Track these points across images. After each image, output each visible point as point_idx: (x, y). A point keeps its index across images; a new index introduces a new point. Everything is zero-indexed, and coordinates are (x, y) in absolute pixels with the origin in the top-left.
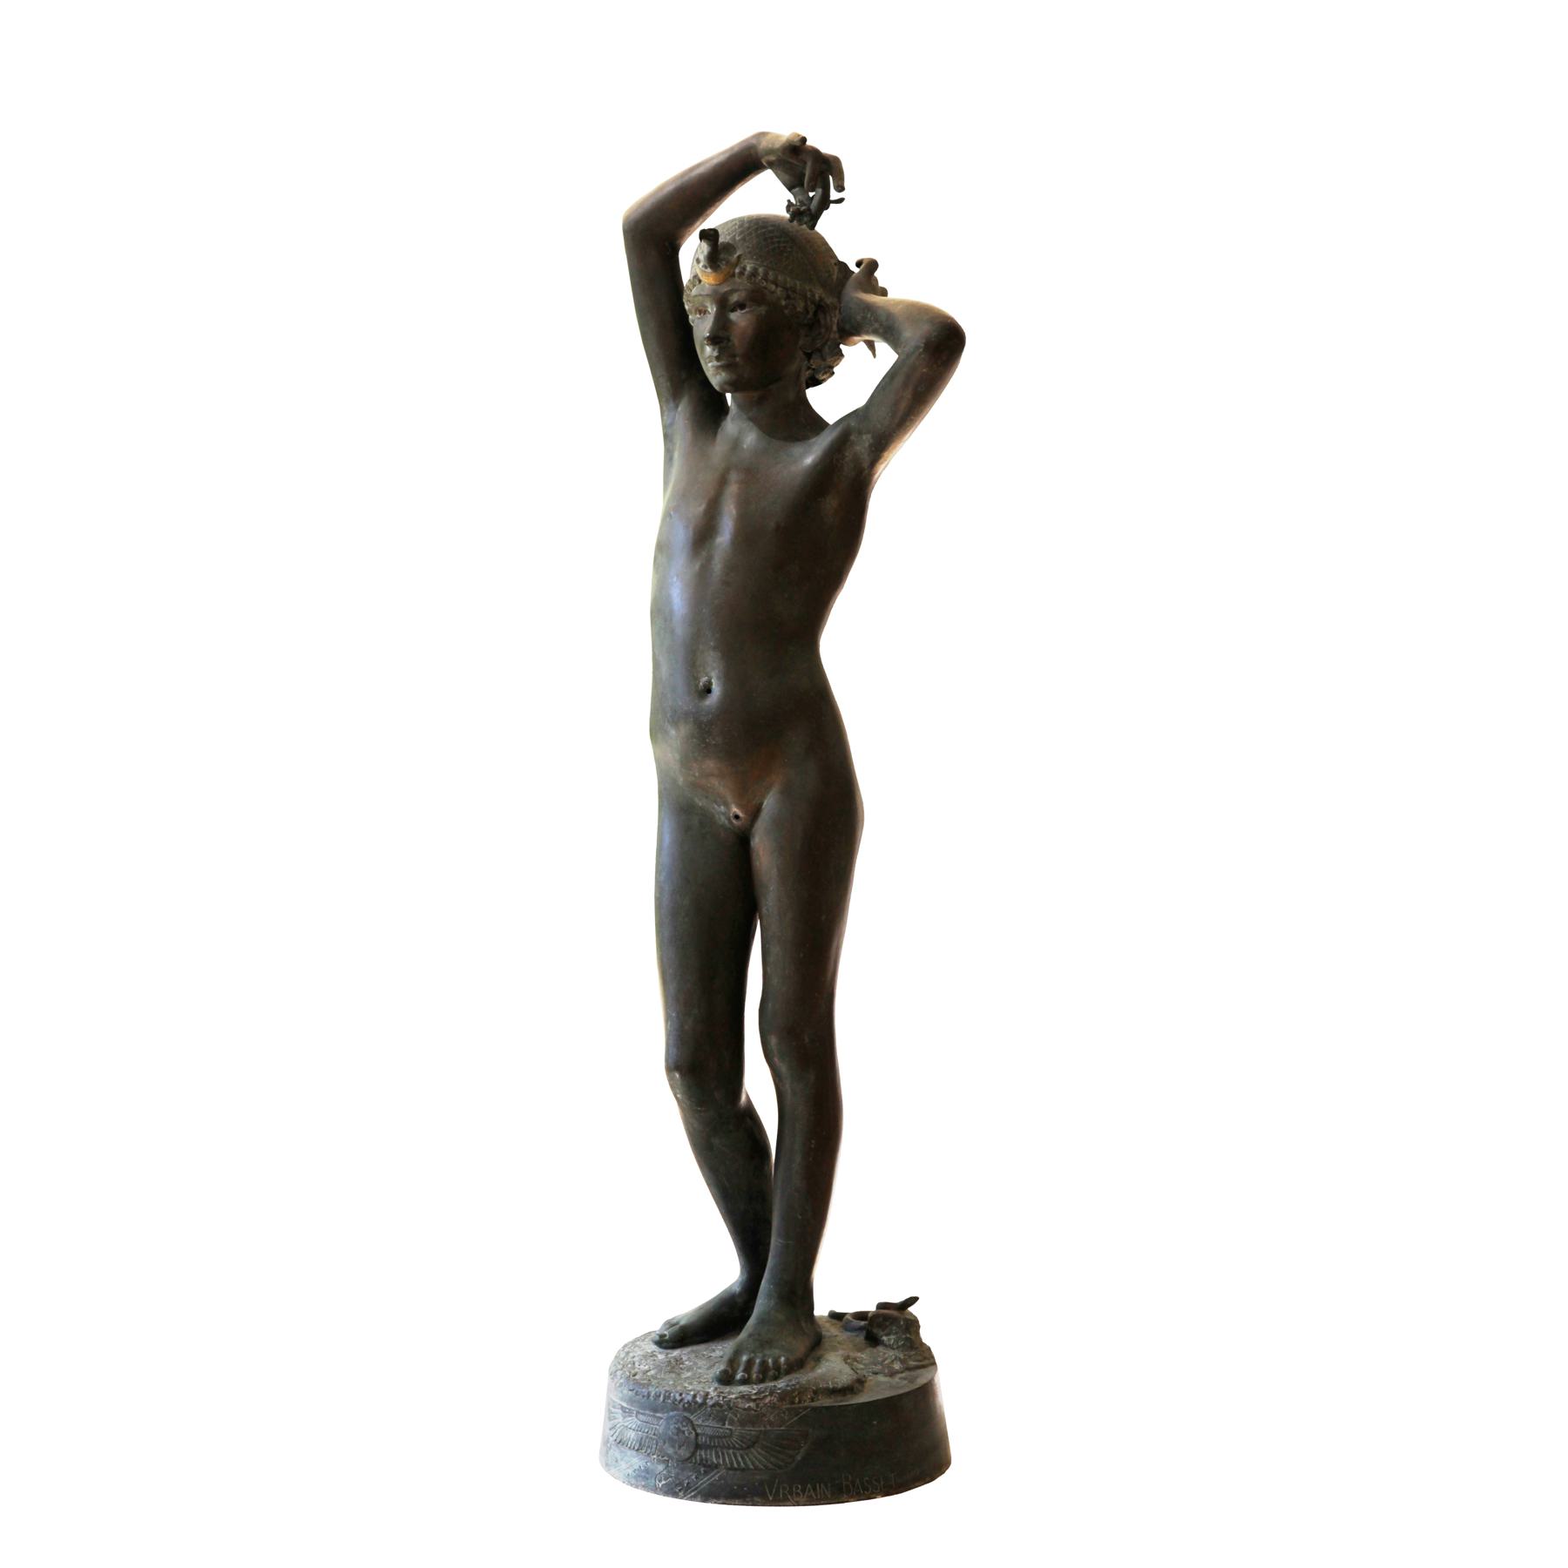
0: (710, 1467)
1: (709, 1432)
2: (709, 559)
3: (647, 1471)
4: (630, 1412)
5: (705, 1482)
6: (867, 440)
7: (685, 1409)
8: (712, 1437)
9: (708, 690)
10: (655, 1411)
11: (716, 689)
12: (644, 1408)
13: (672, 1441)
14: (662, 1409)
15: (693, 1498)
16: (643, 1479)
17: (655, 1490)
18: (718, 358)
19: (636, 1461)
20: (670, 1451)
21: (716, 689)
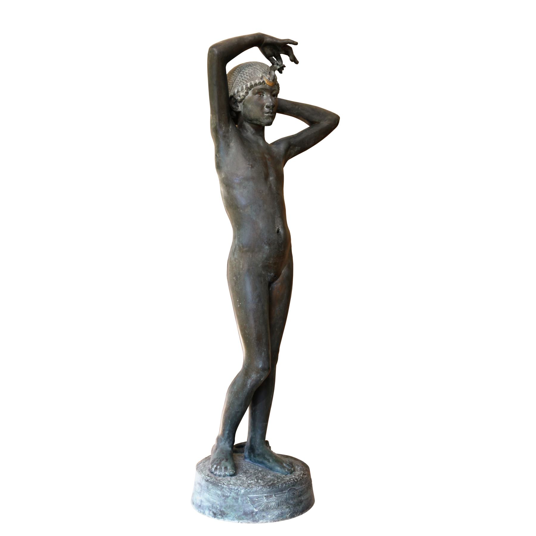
0: (301, 502)
2: (271, 185)
3: (282, 513)
4: (271, 496)
5: (300, 508)
6: (297, 148)
7: (293, 486)
8: (301, 492)
9: (278, 231)
10: (282, 491)
12: (277, 492)
13: (292, 499)
14: (285, 488)
15: (299, 515)
16: (282, 517)
17: (286, 518)
18: (272, 113)
20: (292, 502)
21: (281, 231)
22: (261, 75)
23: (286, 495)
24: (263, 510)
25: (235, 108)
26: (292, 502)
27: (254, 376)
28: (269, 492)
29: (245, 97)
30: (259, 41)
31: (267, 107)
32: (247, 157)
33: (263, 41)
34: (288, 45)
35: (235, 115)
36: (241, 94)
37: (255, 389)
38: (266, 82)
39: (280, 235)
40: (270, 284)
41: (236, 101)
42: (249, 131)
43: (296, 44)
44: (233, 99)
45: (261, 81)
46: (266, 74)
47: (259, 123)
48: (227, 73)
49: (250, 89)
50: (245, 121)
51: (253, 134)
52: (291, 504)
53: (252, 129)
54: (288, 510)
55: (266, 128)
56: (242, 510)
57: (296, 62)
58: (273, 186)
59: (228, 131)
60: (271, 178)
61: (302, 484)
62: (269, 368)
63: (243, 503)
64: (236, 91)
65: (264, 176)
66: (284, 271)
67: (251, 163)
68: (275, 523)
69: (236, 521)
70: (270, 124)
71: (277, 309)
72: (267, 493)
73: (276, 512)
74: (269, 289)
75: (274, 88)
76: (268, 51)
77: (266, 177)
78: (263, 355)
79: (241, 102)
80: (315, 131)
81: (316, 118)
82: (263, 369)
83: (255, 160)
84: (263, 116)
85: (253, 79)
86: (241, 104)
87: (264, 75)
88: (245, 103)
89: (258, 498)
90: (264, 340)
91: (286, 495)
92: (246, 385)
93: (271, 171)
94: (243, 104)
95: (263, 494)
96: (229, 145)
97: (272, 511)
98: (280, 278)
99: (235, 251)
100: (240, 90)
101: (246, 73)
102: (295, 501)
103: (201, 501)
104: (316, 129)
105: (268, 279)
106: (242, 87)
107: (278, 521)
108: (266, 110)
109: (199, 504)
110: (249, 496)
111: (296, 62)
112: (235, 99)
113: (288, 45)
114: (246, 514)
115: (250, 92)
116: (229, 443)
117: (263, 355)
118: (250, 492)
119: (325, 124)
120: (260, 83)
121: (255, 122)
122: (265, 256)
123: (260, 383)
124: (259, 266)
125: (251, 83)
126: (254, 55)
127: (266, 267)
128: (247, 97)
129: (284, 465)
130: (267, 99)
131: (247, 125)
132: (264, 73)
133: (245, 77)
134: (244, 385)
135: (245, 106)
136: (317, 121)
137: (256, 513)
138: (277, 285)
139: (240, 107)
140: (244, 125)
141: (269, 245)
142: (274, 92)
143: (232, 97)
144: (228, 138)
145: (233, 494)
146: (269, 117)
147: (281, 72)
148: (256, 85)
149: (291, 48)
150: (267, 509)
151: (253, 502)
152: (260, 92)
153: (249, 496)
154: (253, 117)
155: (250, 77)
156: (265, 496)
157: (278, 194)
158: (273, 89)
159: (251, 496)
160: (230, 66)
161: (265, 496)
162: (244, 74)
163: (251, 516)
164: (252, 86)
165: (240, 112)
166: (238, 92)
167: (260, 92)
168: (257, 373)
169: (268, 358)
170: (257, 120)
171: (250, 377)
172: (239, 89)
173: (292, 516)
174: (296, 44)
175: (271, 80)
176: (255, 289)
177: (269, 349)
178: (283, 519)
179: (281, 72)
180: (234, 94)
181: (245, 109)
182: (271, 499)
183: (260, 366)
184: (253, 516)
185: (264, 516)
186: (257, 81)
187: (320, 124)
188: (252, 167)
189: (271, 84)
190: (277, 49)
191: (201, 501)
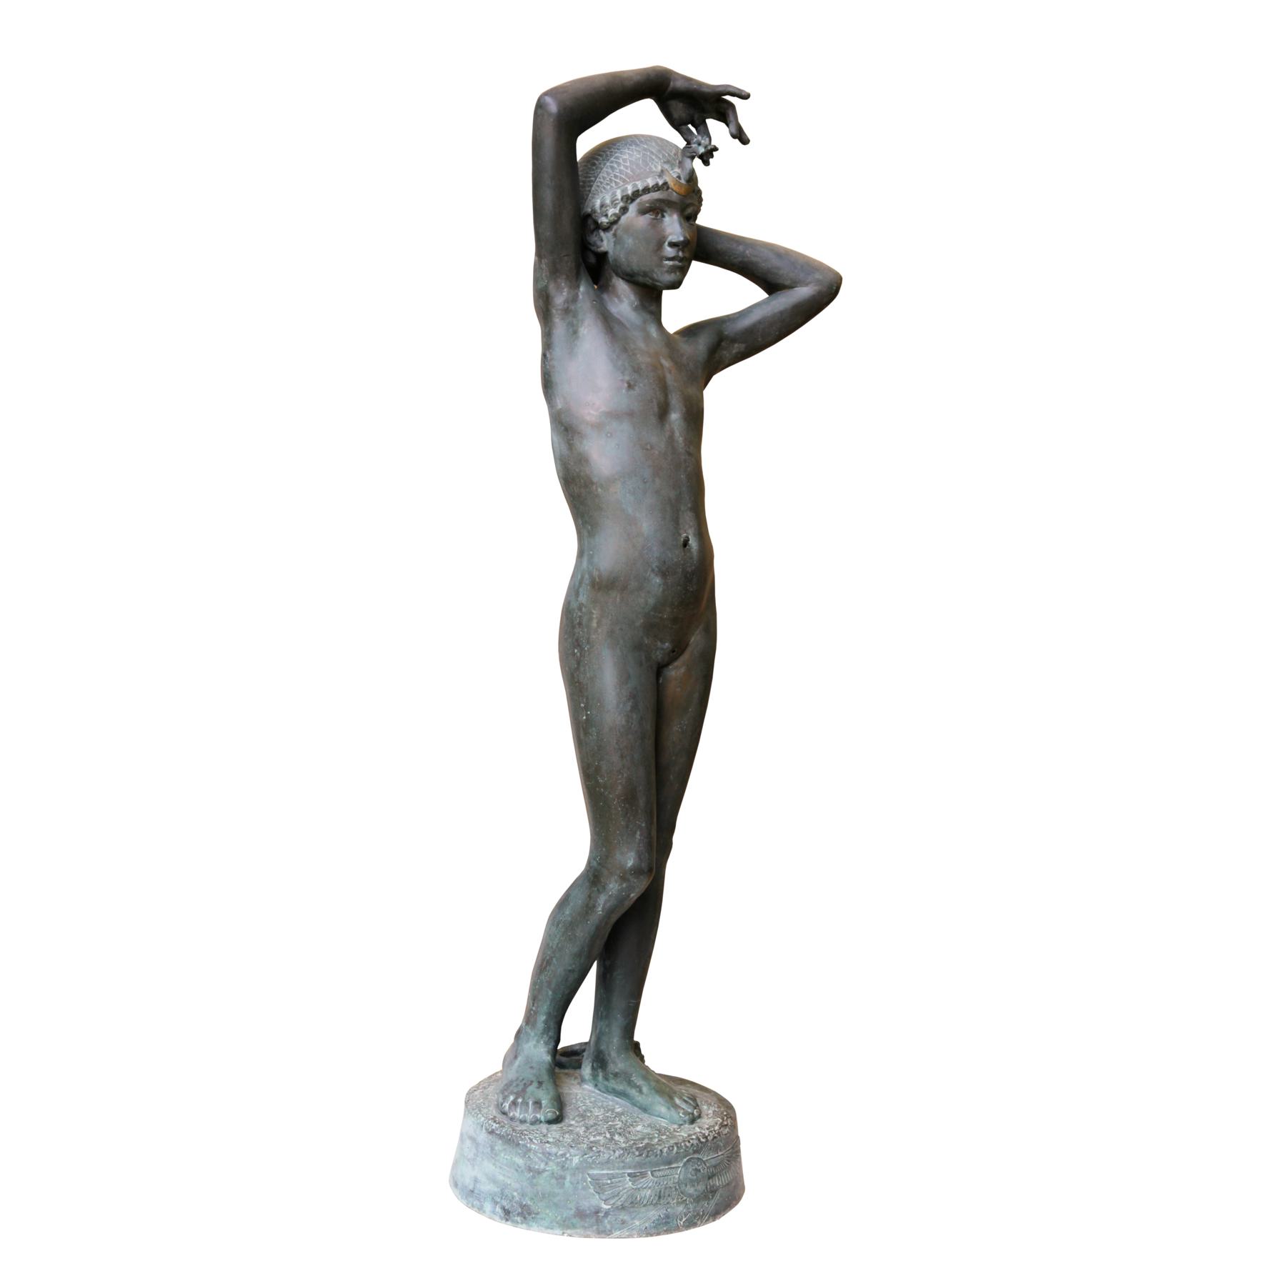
1: (713, 1162)
2: (672, 432)
3: (667, 1216)
4: (643, 1175)
5: (710, 1206)
6: (737, 348)
7: (695, 1152)
8: (715, 1167)
9: (686, 543)
10: (670, 1163)
11: (693, 543)
12: (657, 1164)
14: (677, 1158)
15: (707, 1221)
16: (666, 1226)
17: (677, 1229)
18: (681, 260)
19: (654, 1214)
20: (691, 1190)
21: (693, 543)
22: (659, 168)
23: (679, 1172)
24: (623, 1208)
25: (595, 244)
26: (691, 1190)
27: (613, 887)
28: (640, 1165)
29: (619, 218)
30: (659, 87)
31: (672, 245)
32: (620, 363)
33: (668, 85)
34: (727, 97)
35: (592, 260)
36: (611, 211)
37: (614, 918)
38: (671, 184)
39: (689, 550)
40: (660, 669)
41: (598, 226)
42: (623, 302)
43: (745, 96)
44: (590, 222)
45: (661, 183)
46: (672, 166)
47: (649, 282)
48: (578, 159)
49: (633, 200)
50: (618, 275)
51: (636, 309)
52: (690, 1196)
53: (632, 297)
54: (681, 1208)
55: (666, 294)
56: (572, 1206)
57: (744, 140)
58: (677, 434)
59: (574, 299)
60: (675, 417)
61: (717, 1148)
62: (650, 870)
63: (576, 1189)
64: (598, 203)
65: (656, 409)
66: (696, 639)
67: (627, 378)
68: (650, 1238)
69: (559, 1231)
70: (676, 285)
71: (675, 729)
72: (635, 1167)
73: (654, 1214)
74: (658, 679)
75: (688, 200)
76: (679, 109)
77: (663, 412)
78: (638, 836)
79: (606, 229)
80: (782, 308)
81: (785, 273)
82: (637, 871)
83: (637, 370)
84: (661, 265)
85: (639, 178)
86: (610, 234)
87: (666, 166)
88: (619, 232)
89: (611, 1177)
90: (642, 802)
91: (679, 1172)
92: (594, 906)
93: (675, 400)
94: (615, 235)
95: (624, 1168)
96: (575, 332)
97: (643, 1209)
98: (686, 656)
99: (581, 583)
100: (608, 202)
101: (625, 161)
102: (701, 1187)
103: (476, 1180)
104: (785, 300)
105: (658, 656)
106: (614, 194)
107: (658, 1234)
108: (669, 251)
109: (471, 1187)
110: (591, 1172)
111: (744, 140)
112: (596, 222)
113: (727, 97)
114: (581, 1214)
115: (633, 208)
116: (546, 1043)
117: (638, 836)
118: (594, 1162)
119: (803, 292)
120: (657, 188)
121: (641, 279)
122: (651, 601)
123: (628, 904)
124: (638, 624)
125: (635, 185)
126: (643, 119)
127: (652, 627)
128: (624, 218)
129: (677, 1101)
130: (673, 227)
131: (621, 286)
132: (668, 162)
133: (621, 172)
134: (589, 908)
135: (618, 240)
136: (787, 283)
137: (607, 1214)
138: (675, 672)
139: (605, 243)
140: (614, 287)
141: (664, 574)
142: (689, 210)
143: (589, 216)
144: (575, 316)
145: (552, 1167)
146: (672, 269)
147: (706, 163)
148: (647, 190)
149: (732, 106)
150: (632, 1204)
151: (600, 1188)
152: (656, 210)
153: (591, 1172)
154: (635, 268)
155: (632, 170)
156: (629, 1175)
157: (689, 454)
158: (689, 201)
159: (595, 1172)
160: (586, 143)
161: (629, 1175)
162: (619, 164)
163: (593, 1220)
164: (636, 194)
165: (605, 254)
166: (602, 206)
167: (656, 210)
168: (623, 879)
169: (650, 845)
170: (645, 274)
171: (604, 888)
172: (606, 197)
173: (691, 1224)
174: (745, 96)
175: (683, 181)
176: (624, 678)
177: (652, 823)
178: (669, 1231)
179: (706, 163)
180: (594, 211)
181: (618, 247)
182: (642, 1182)
183: (630, 863)
184: (598, 1221)
185: (623, 1222)
186: (650, 182)
187: (795, 293)
188: (630, 387)
189: (682, 191)
190: (696, 106)
191: (476, 1180)
